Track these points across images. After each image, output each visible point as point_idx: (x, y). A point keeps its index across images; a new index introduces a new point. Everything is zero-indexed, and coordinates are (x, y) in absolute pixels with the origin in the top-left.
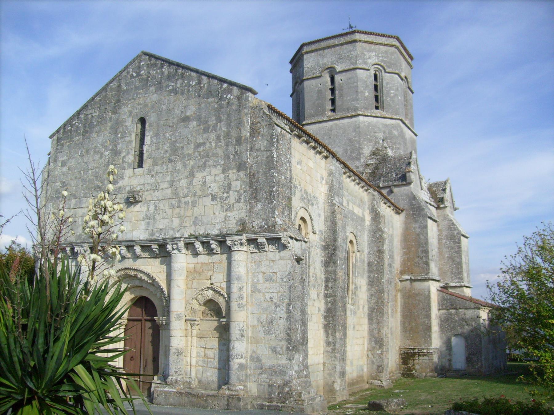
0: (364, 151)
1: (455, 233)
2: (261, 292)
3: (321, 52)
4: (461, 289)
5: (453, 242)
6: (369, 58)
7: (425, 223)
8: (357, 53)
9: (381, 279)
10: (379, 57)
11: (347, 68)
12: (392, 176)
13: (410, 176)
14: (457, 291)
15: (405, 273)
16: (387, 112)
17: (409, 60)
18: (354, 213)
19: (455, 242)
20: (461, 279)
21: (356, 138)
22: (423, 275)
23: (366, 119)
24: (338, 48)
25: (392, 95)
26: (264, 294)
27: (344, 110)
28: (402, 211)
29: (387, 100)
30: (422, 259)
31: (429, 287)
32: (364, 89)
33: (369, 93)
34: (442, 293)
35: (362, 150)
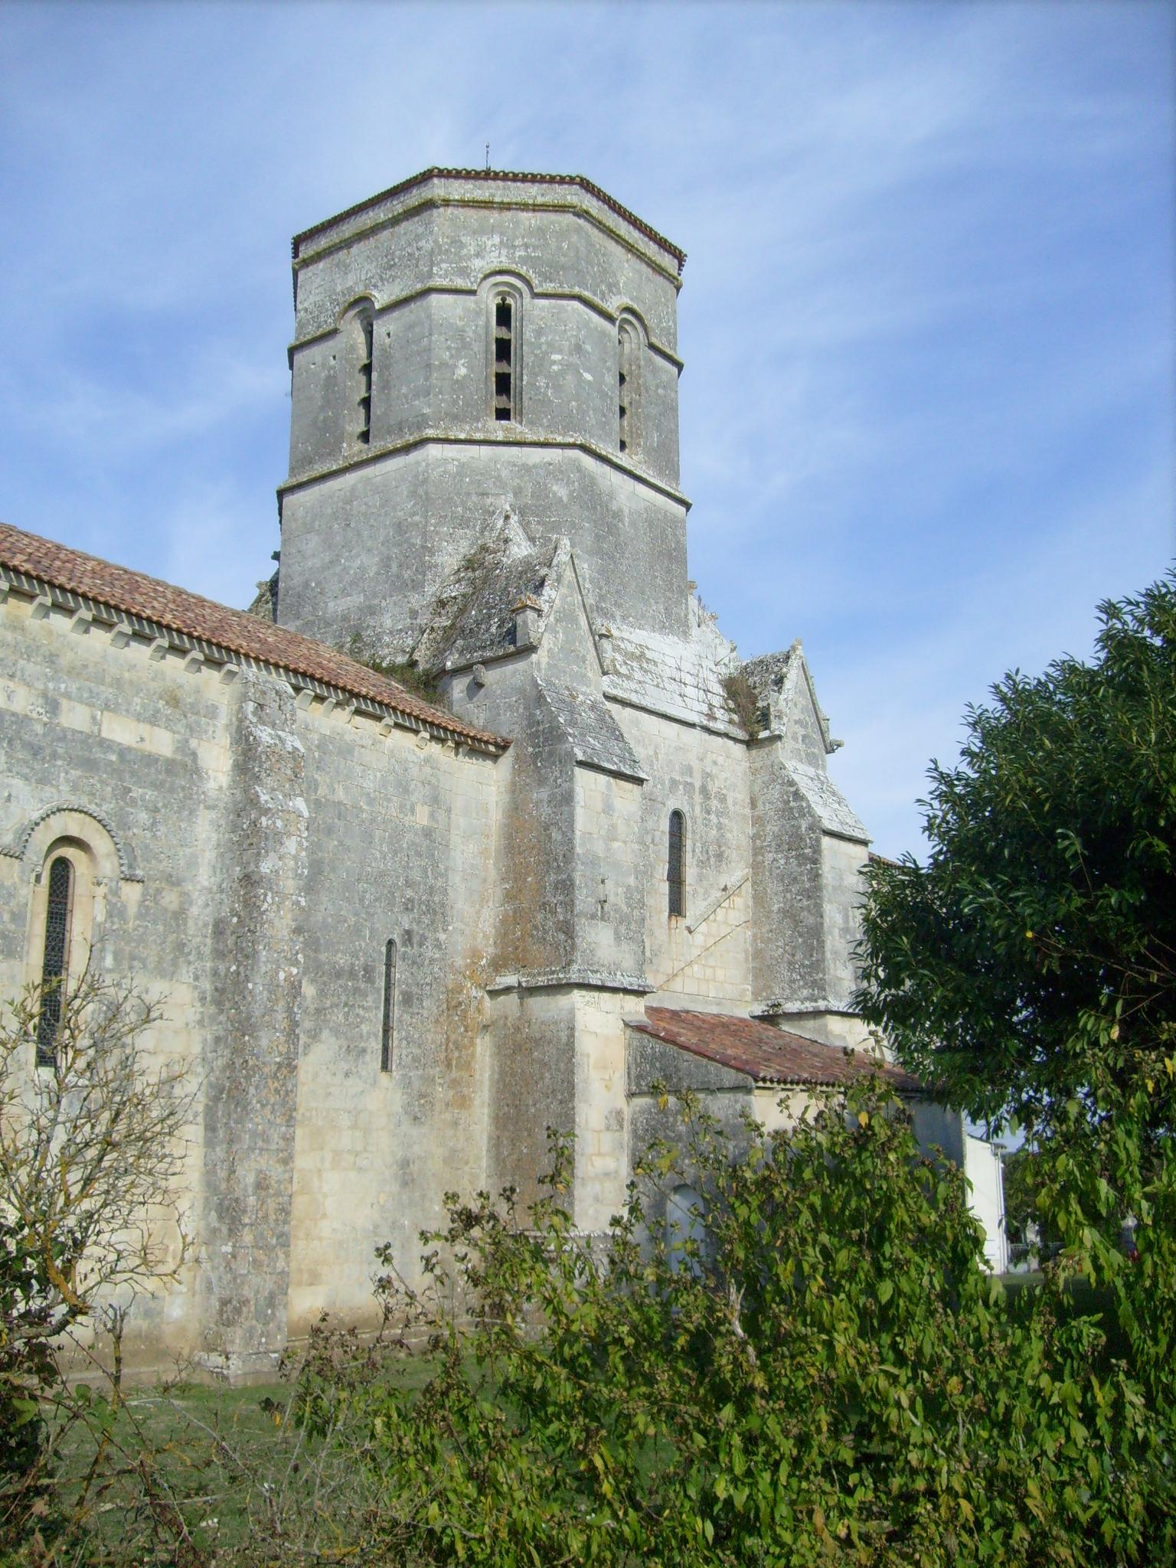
0: (438, 559)
1: (804, 825)
3: (342, 255)
4: (819, 1022)
5: (797, 857)
6: (478, 255)
7: (566, 785)
8: (436, 242)
9: (247, 979)
10: (514, 247)
11: (404, 294)
12: (488, 630)
13: (525, 623)
14: (806, 1030)
15: (505, 966)
16: (531, 423)
17: (667, 261)
18: (105, 745)
19: (802, 859)
20: (819, 987)
21: (417, 518)
22: (553, 973)
23: (450, 451)
24: (386, 234)
25: (555, 368)
27: (389, 432)
28: (503, 747)
29: (527, 379)
30: (554, 913)
31: (572, 1012)
32: (452, 356)
33: (471, 368)
34: (638, 1035)
35: (432, 555)
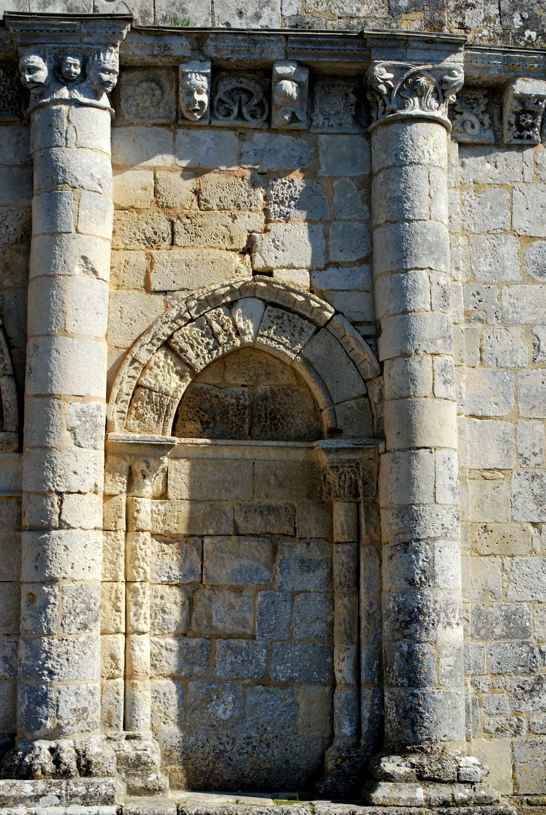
2: (516, 323)
26: (529, 329)
